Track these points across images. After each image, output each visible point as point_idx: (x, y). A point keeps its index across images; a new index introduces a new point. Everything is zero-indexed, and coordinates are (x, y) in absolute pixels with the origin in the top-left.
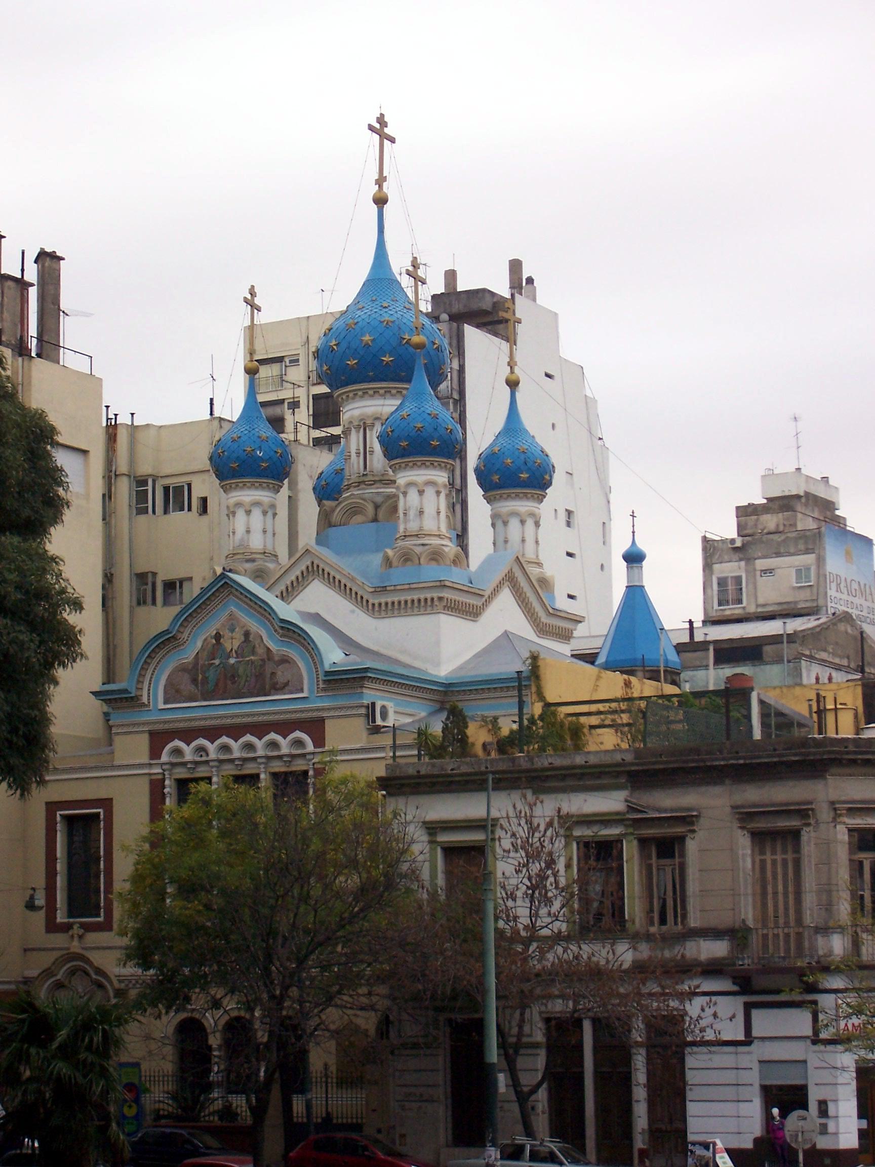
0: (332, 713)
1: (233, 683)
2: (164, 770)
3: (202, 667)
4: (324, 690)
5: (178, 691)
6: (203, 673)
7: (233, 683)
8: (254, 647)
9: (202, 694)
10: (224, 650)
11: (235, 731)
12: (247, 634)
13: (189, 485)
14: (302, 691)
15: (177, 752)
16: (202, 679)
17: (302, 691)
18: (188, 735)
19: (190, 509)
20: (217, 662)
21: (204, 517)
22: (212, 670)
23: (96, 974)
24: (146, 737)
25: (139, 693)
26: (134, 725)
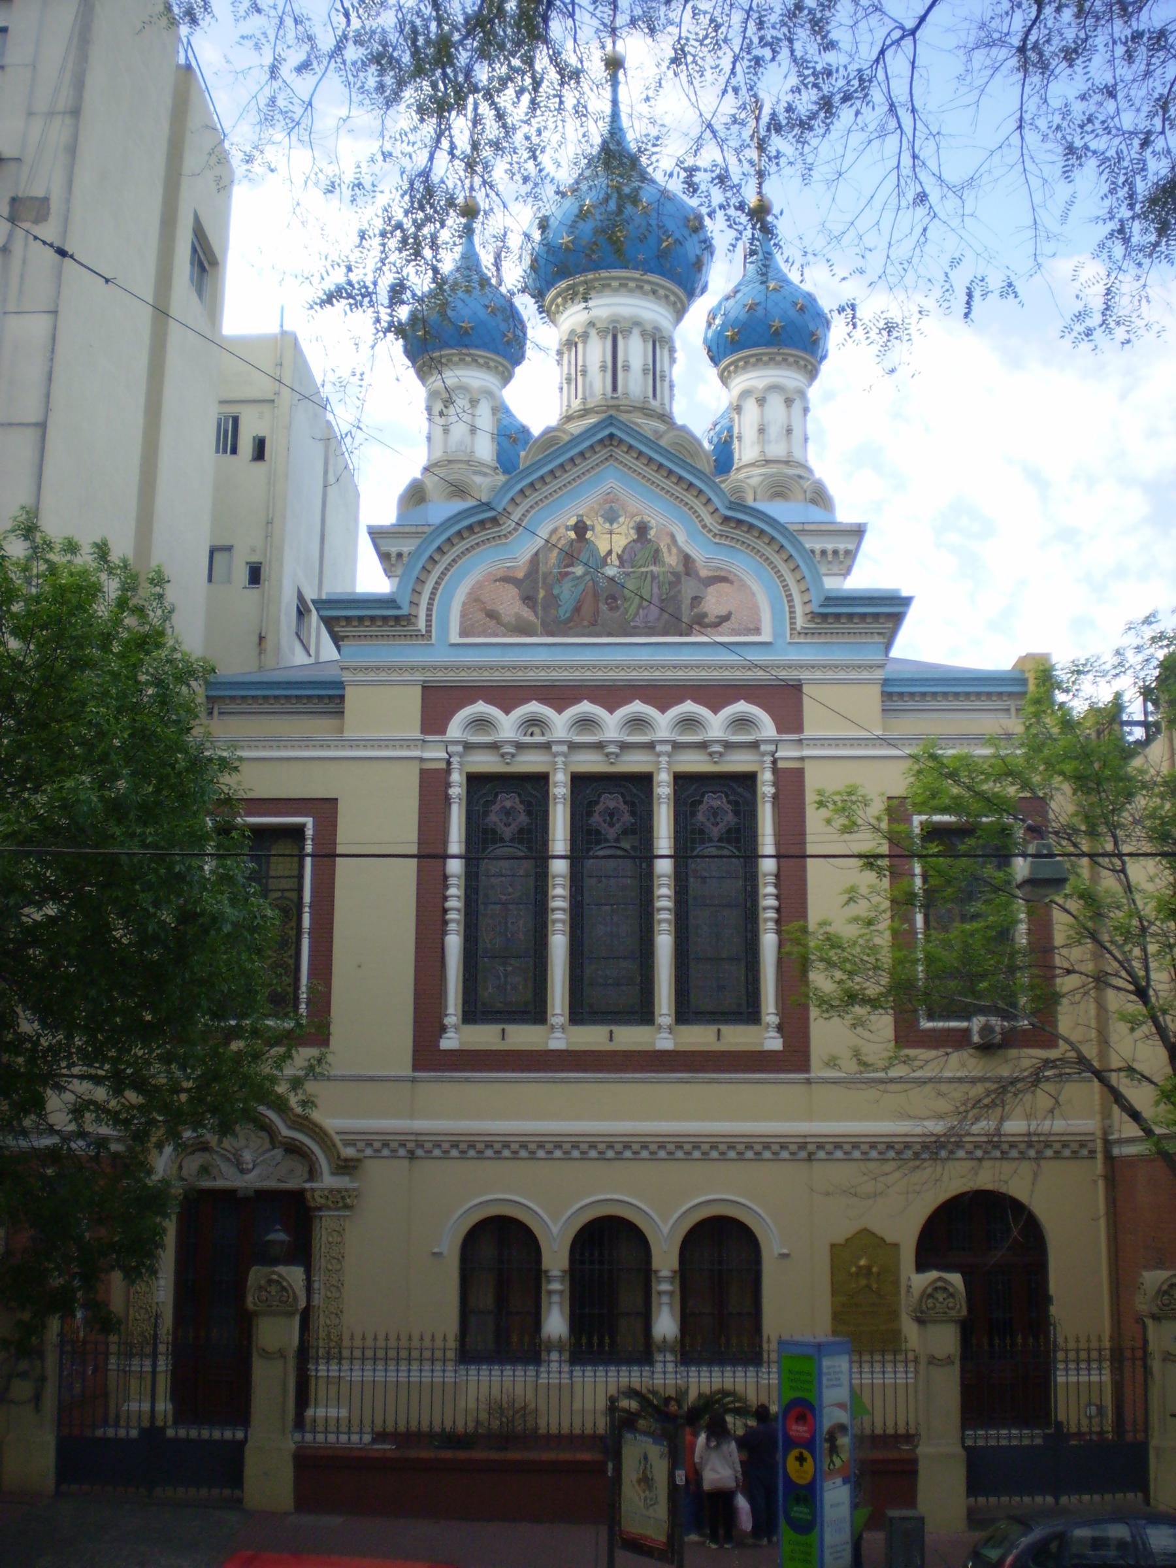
0: (818, 675)
3: (545, 579)
4: (805, 633)
5: (492, 615)
6: (549, 589)
8: (657, 551)
9: (543, 624)
10: (594, 551)
11: (611, 695)
12: (642, 530)
13: (236, 420)
15: (481, 723)
16: (544, 597)
17: (757, 631)
18: (507, 696)
20: (579, 570)
22: (567, 585)
23: (289, 1128)
24: (418, 691)
26: (390, 669)
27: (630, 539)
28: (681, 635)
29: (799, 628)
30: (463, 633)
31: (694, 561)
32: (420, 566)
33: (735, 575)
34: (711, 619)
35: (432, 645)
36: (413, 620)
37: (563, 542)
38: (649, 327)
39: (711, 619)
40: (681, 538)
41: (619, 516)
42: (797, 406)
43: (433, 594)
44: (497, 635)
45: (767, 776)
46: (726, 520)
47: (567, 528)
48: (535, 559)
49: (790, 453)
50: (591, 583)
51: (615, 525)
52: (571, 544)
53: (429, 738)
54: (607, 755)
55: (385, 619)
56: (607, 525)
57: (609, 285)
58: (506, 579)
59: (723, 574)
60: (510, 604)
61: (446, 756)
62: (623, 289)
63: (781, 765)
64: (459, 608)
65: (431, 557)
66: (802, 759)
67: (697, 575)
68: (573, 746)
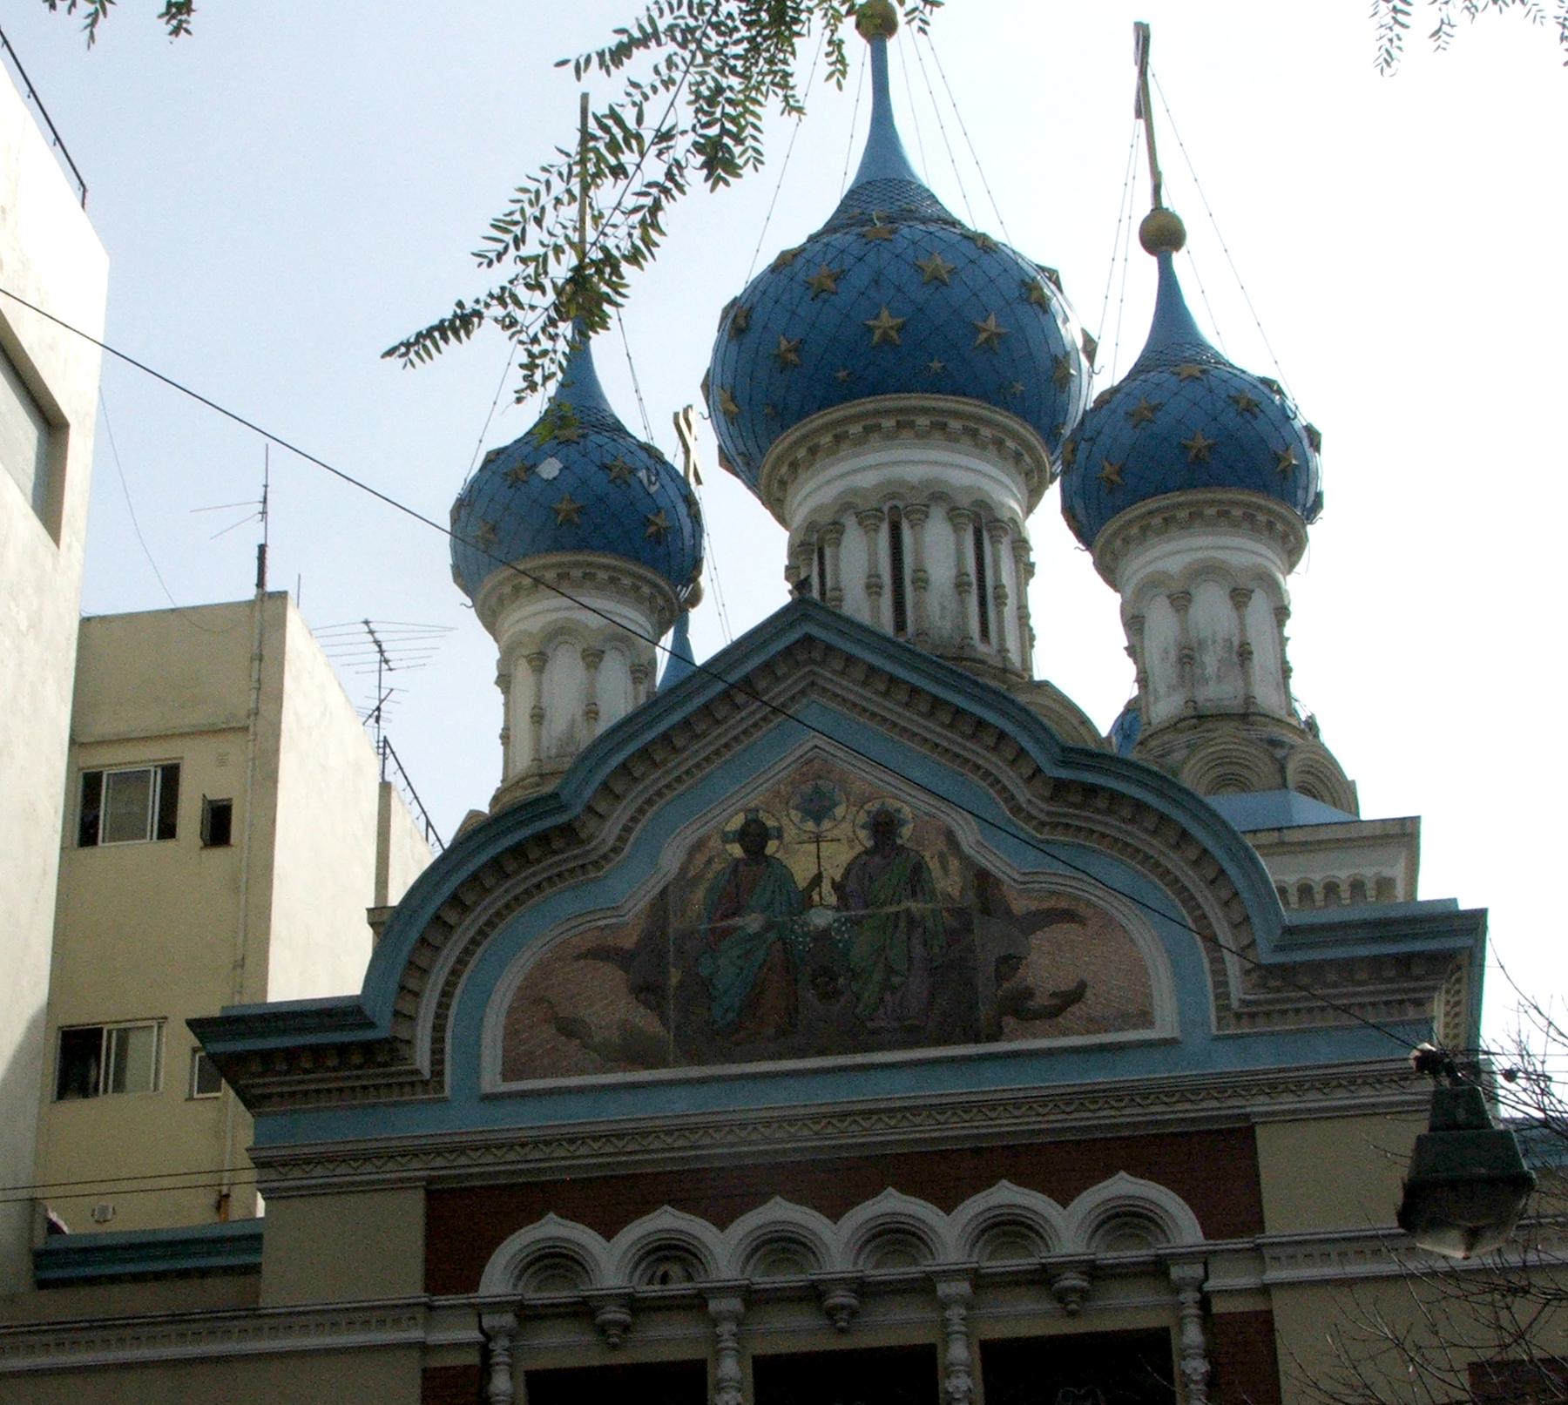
1: (829, 996)
2: (488, 1336)
5: (569, 1028)
7: (829, 996)
8: (919, 869)
12: (884, 827)
14: (1150, 1024)
15: (556, 1262)
16: (681, 984)
17: (1145, 1018)
18: (609, 1198)
19: (167, 830)
20: (752, 922)
21: (218, 853)
24: (414, 1206)
25: (403, 1033)
27: (859, 849)
28: (977, 1041)
29: (1235, 1004)
30: (509, 1073)
31: (998, 882)
32: (414, 935)
33: (1088, 903)
34: (1041, 1000)
35: (445, 1100)
36: (404, 1050)
37: (717, 866)
38: (964, 501)
39: (1041, 1000)
40: (968, 835)
41: (835, 805)
42: (1259, 604)
43: (446, 994)
44: (582, 1072)
45: (1193, 1335)
46: (1060, 788)
47: (726, 838)
48: (660, 905)
49: (1249, 699)
50: (779, 946)
51: (826, 824)
52: (735, 871)
53: (441, 1300)
54: (830, 1313)
55: (342, 1050)
56: (810, 825)
57: (878, 427)
58: (602, 954)
59: (1064, 905)
60: (608, 1003)
61: (475, 1335)
62: (906, 434)
63: (1219, 1306)
64: (502, 1020)
65: (437, 918)
66: (1265, 1290)
67: (1008, 912)
68: (753, 1298)
